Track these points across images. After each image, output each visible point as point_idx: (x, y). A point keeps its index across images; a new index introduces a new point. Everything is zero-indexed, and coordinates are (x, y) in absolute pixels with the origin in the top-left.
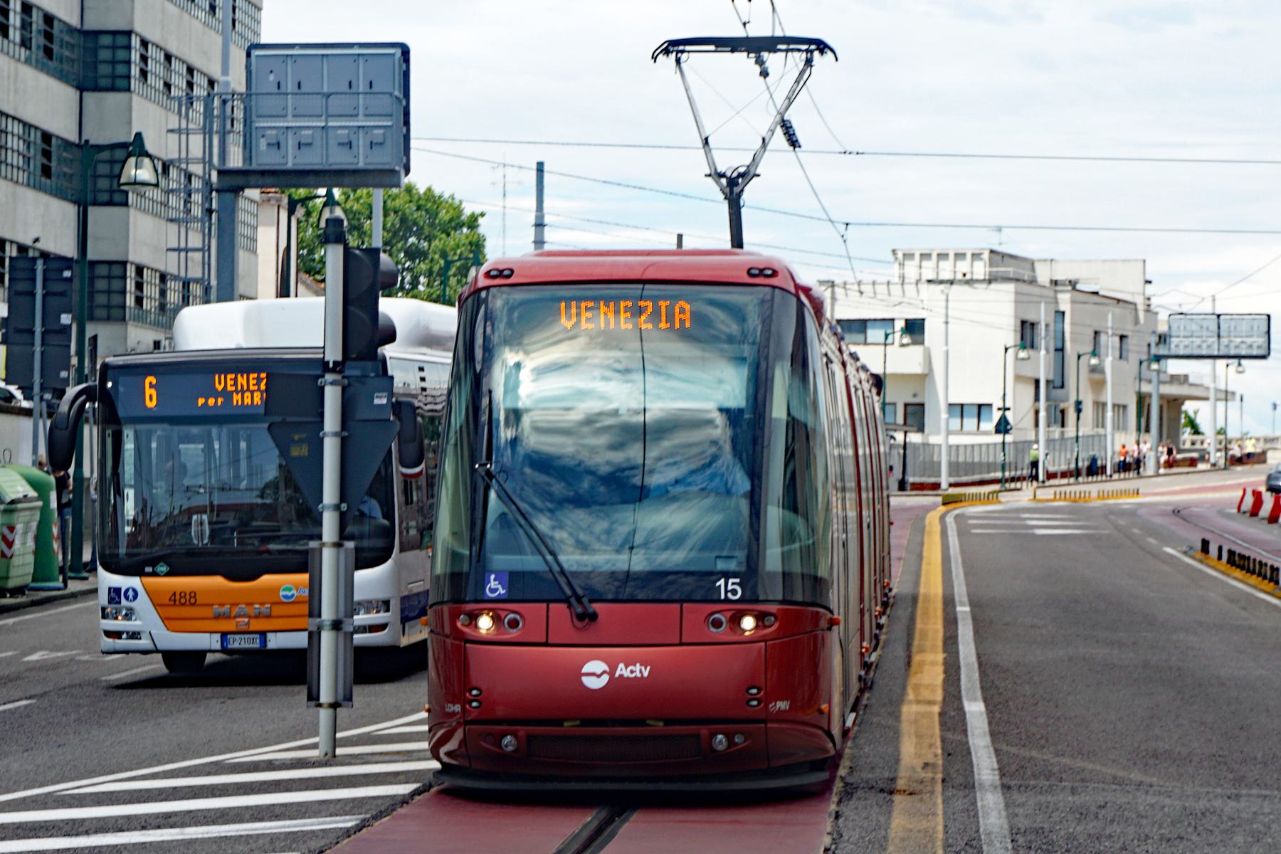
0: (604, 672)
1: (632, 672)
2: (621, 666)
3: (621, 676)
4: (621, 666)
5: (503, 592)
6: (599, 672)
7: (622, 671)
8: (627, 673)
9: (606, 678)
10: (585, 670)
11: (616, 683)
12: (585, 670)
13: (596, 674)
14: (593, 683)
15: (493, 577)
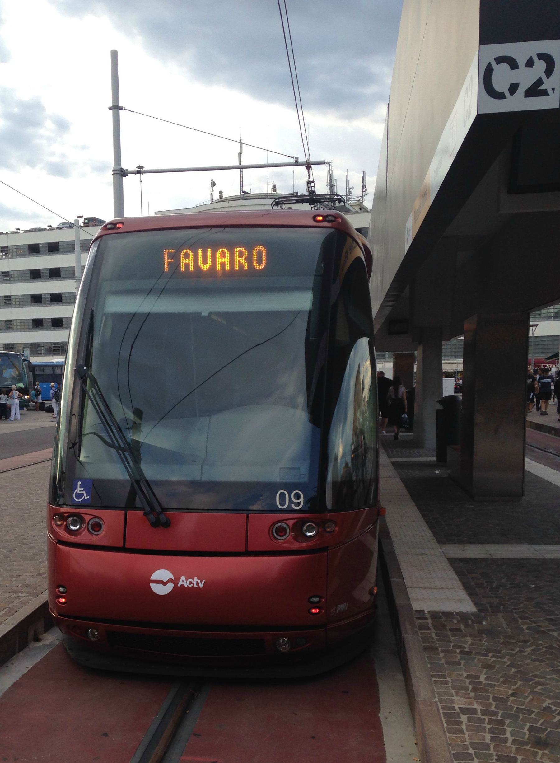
0: (170, 580)
1: (190, 583)
2: (183, 578)
3: (183, 586)
4: (183, 578)
5: (86, 498)
6: (165, 580)
7: (184, 582)
8: (186, 584)
9: (171, 586)
10: (152, 578)
11: (178, 591)
12: (152, 578)
13: (162, 579)
14: (160, 590)
15: (79, 483)
